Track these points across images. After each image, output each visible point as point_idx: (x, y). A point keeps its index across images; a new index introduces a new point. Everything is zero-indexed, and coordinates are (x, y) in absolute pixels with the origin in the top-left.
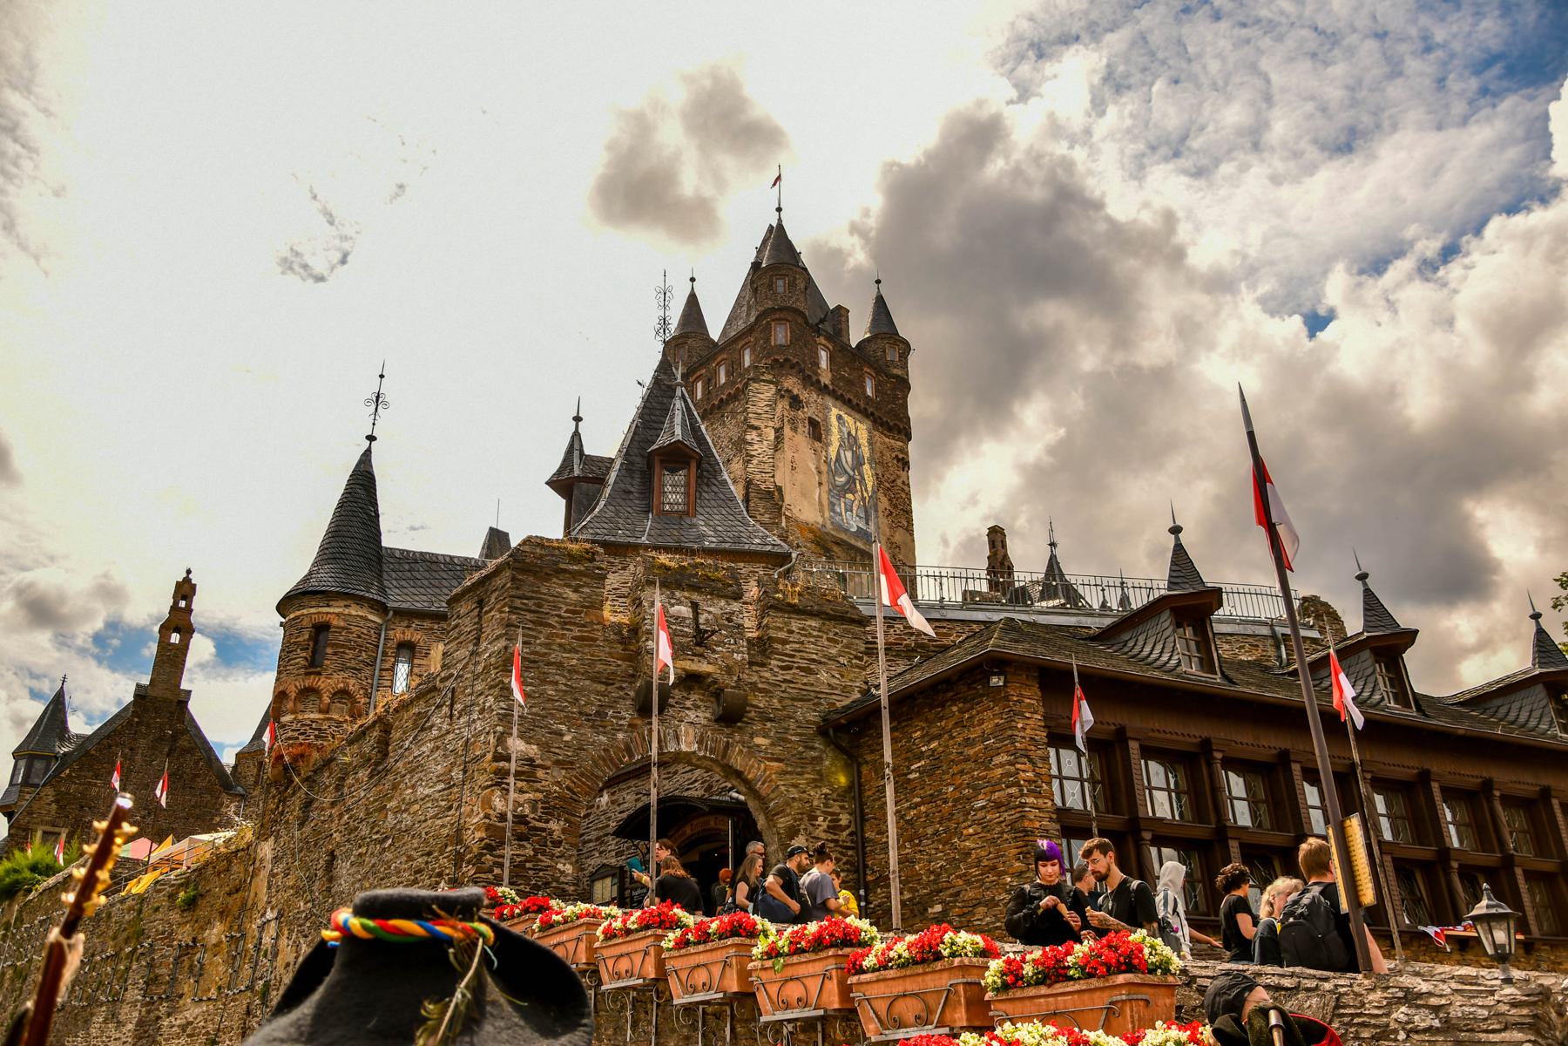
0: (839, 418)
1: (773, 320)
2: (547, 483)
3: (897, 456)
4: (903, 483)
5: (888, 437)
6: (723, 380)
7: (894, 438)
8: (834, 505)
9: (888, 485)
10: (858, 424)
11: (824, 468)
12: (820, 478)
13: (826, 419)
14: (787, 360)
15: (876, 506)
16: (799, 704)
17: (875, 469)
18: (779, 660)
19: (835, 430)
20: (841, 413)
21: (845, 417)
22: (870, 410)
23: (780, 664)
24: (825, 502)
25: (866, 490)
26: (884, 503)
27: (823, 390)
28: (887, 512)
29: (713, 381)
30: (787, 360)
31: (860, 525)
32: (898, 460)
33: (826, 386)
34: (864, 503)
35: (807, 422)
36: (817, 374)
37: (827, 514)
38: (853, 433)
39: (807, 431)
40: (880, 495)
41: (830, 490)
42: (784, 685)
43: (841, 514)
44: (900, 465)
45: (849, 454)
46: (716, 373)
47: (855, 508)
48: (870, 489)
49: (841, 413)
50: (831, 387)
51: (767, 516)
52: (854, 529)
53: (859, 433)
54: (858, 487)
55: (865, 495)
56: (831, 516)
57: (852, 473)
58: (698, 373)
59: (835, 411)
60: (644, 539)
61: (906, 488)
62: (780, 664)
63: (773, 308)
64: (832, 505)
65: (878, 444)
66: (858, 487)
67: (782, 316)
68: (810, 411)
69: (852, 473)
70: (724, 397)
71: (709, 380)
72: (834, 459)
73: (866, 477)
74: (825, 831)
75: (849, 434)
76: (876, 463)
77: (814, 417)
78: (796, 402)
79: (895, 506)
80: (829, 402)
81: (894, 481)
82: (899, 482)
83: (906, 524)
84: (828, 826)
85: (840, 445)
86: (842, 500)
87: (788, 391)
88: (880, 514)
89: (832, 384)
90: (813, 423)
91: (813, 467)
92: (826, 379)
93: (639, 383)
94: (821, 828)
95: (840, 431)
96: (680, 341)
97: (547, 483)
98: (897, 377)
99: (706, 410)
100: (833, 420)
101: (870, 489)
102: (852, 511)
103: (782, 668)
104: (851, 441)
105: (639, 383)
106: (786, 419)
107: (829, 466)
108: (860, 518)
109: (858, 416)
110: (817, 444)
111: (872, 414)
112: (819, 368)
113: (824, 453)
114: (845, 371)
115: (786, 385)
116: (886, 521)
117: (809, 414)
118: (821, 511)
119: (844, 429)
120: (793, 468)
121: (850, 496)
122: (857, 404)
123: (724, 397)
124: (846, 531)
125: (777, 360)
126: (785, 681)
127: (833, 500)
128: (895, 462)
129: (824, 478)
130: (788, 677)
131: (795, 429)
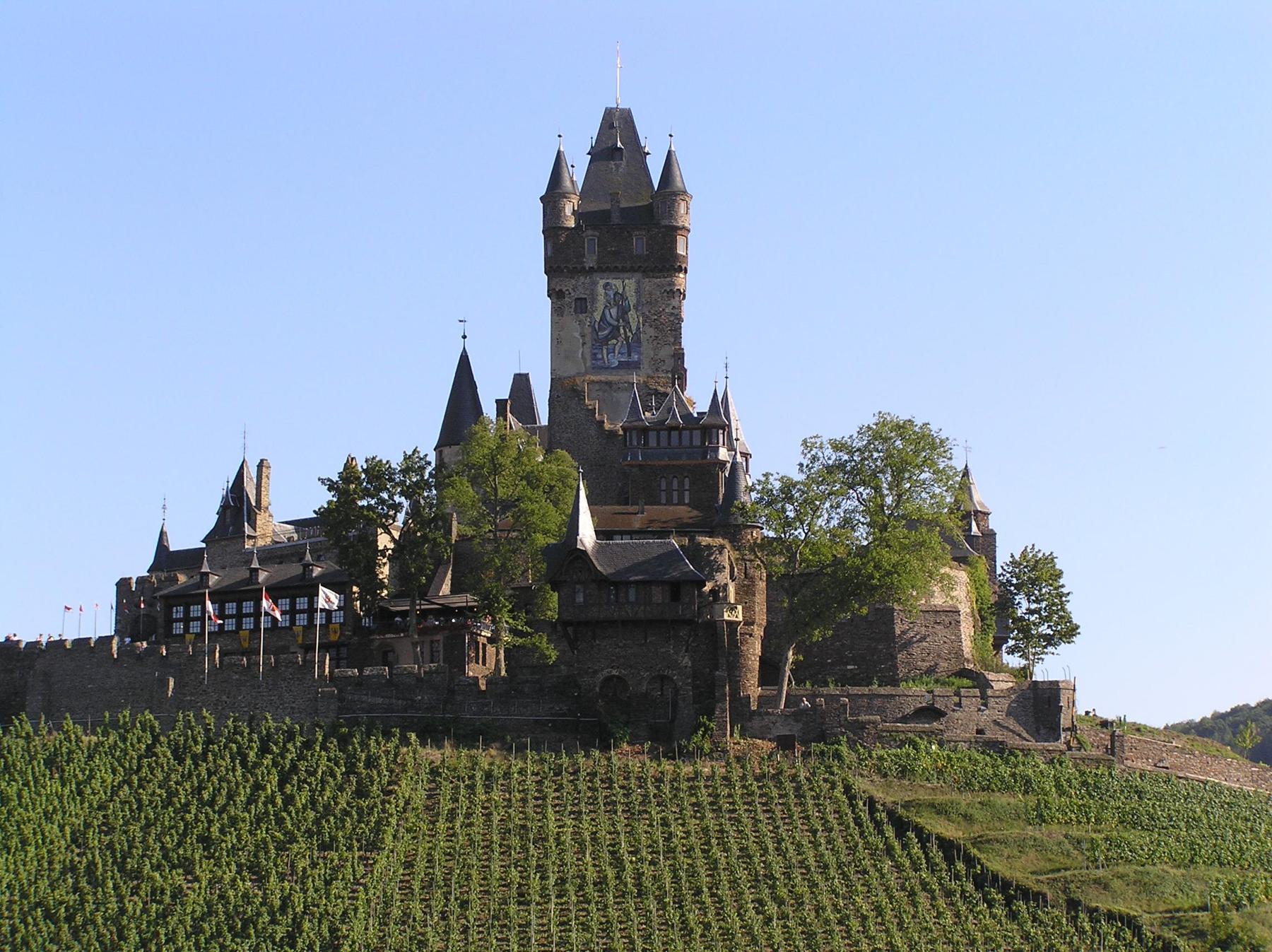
0: (606, 286)
8: (595, 354)
10: (627, 281)
11: (588, 330)
12: (583, 340)
15: (639, 339)
21: (614, 282)
24: (588, 357)
25: (630, 331)
33: (591, 268)
34: (627, 342)
44: (671, 295)
45: (614, 311)
50: (596, 267)
53: (627, 288)
54: (622, 331)
55: (629, 334)
59: (602, 282)
61: (675, 311)
64: (594, 356)
66: (622, 331)
72: (598, 320)
73: (631, 320)
75: (616, 294)
80: (596, 277)
88: (645, 344)
91: (577, 335)
93: (460, 321)
98: (666, 227)
100: (601, 290)
102: (614, 352)
104: (620, 298)
105: (460, 321)
110: (582, 316)
118: (585, 364)
128: (665, 294)
129: (588, 339)
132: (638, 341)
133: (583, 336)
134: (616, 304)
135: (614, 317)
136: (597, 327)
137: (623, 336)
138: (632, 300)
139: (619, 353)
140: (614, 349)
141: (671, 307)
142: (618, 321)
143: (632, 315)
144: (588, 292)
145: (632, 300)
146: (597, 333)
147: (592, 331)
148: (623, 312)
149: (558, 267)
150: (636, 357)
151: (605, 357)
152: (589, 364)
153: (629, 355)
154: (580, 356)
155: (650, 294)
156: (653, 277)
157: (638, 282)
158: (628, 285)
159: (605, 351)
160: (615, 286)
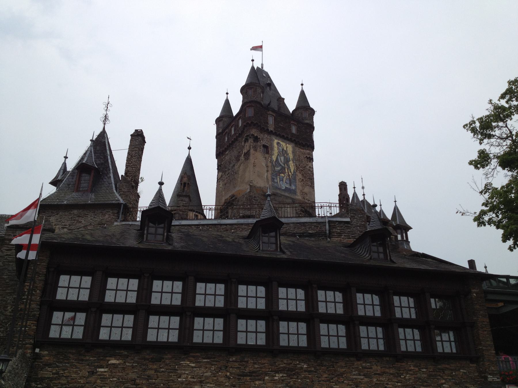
0: (278, 144)
1: (247, 107)
2: (49, 183)
3: (306, 157)
4: (310, 167)
5: (302, 149)
6: (233, 133)
7: (305, 149)
9: (302, 169)
10: (288, 145)
11: (270, 164)
12: (267, 169)
13: (272, 145)
14: (252, 123)
16: (11, 264)
17: (295, 163)
18: (7, 247)
19: (276, 149)
20: (279, 141)
21: (282, 143)
22: (293, 139)
23: (5, 248)
24: (270, 179)
25: (291, 172)
26: (299, 176)
27: (270, 133)
28: (301, 180)
29: (230, 134)
30: (252, 123)
31: (287, 186)
32: (307, 158)
33: (271, 131)
34: (289, 177)
35: (262, 147)
36: (267, 127)
37: (270, 183)
38: (285, 150)
39: (261, 150)
40: (298, 173)
41: (272, 173)
42: (6, 257)
43: (277, 182)
44: (308, 160)
45: (282, 158)
46: (231, 131)
47: (284, 179)
48: (292, 171)
49: (279, 141)
50: (274, 131)
51: (126, 189)
52: (284, 188)
53: (288, 149)
54: (287, 171)
55: (290, 174)
56: (272, 184)
57: (283, 165)
58: (226, 131)
59: (276, 141)
60: (65, 202)
61: (311, 169)
62: (5, 248)
63: (247, 102)
64: (273, 180)
65: (297, 153)
66: (287, 171)
67: (250, 105)
68: (263, 142)
69: (283, 165)
70: (233, 140)
71: (229, 133)
72: (275, 160)
73: (291, 166)
74: (10, 312)
75: (283, 149)
76: (296, 160)
77: (266, 144)
78: (256, 139)
79: (305, 177)
80: (273, 138)
81: (304, 167)
82: (308, 167)
83: (310, 184)
84: (12, 310)
85: (278, 155)
86: (278, 177)
87: (253, 135)
88: (297, 181)
89: (275, 130)
90: (264, 146)
91: (264, 165)
92: (271, 128)
93: (188, 138)
94: (8, 311)
95: (278, 149)
96: (221, 119)
97: (49, 183)
98: (307, 124)
99: (228, 146)
100: (275, 145)
101: (292, 171)
102: (283, 181)
103: (7, 250)
104: (284, 152)
105: (188, 138)
106: (251, 147)
107: (272, 163)
108: (287, 183)
109: (287, 142)
110: (267, 155)
111: (295, 140)
112: (268, 124)
113: (270, 159)
114: (281, 124)
115: (252, 133)
116: (300, 184)
117: (263, 143)
118: (268, 182)
119: (280, 148)
120: (254, 166)
121: (283, 175)
122: (287, 137)
123: (233, 140)
124: (280, 189)
125: (248, 123)
126: (7, 255)
127: (274, 177)
128: (306, 159)
129: (270, 169)
130: (9, 254)
131: (256, 150)
132: (295, 179)
133: (267, 166)
134: (284, 155)
135: (283, 162)
136: (274, 164)
137: (287, 174)
138: (291, 156)
139: (285, 182)
140: (283, 179)
141: (309, 166)
142: (284, 165)
143: (291, 164)
144: (269, 143)
145: (291, 156)
146: (274, 167)
147: (272, 165)
148: (287, 161)
149: (257, 123)
150: (293, 187)
151: (279, 182)
152: (270, 183)
153: (290, 185)
154: (266, 178)
155: (299, 156)
156: (300, 148)
157: (293, 148)
158: (289, 148)
159: (278, 179)
160: (283, 145)
